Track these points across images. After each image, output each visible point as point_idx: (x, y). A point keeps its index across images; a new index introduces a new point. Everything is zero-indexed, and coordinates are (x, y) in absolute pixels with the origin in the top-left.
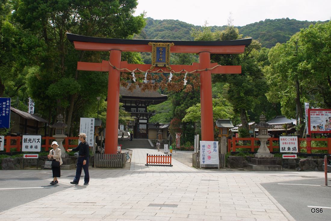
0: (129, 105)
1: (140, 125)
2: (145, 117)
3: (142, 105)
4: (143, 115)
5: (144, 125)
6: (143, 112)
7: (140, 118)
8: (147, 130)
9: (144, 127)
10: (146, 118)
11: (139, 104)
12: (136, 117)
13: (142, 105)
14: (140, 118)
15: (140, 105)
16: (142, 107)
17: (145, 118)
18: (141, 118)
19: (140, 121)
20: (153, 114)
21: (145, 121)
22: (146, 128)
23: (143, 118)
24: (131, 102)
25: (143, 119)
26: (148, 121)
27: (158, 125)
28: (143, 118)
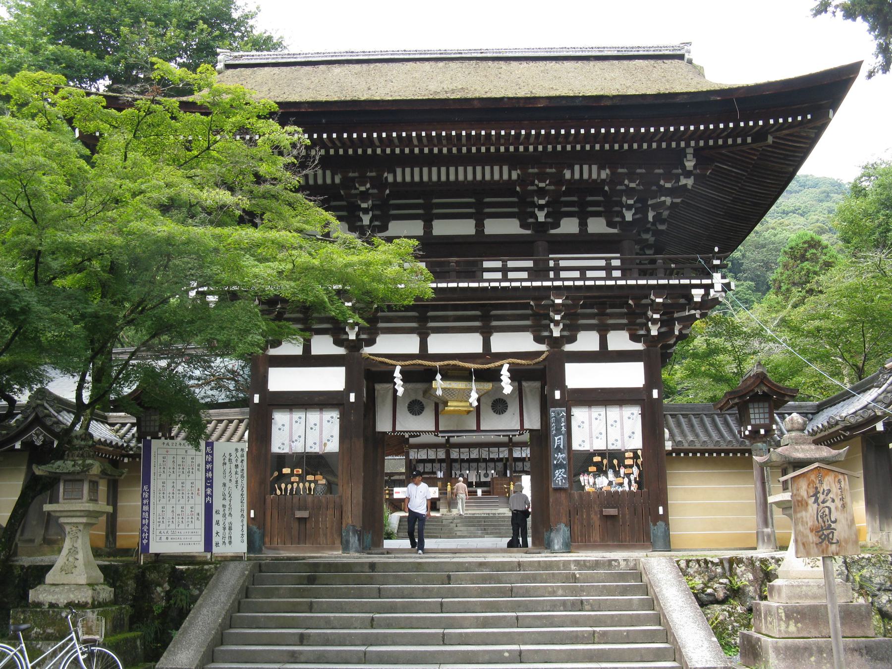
0: (465, 228)
1: (580, 414)
2: (625, 335)
3: (583, 225)
4: (598, 308)
5: (614, 413)
6: (597, 278)
7: (568, 348)
8: (655, 464)
9: (622, 429)
10: (634, 338)
11: (556, 217)
12: (538, 339)
13: (583, 225)
14: (568, 348)
15: (569, 226)
16: (583, 244)
17: (619, 341)
18: (588, 341)
19: (577, 376)
20: (697, 294)
21: (632, 375)
22: (636, 442)
23: (603, 342)
24: (479, 200)
25: (604, 355)
26: (652, 377)
27: (756, 398)
28: (603, 342)
